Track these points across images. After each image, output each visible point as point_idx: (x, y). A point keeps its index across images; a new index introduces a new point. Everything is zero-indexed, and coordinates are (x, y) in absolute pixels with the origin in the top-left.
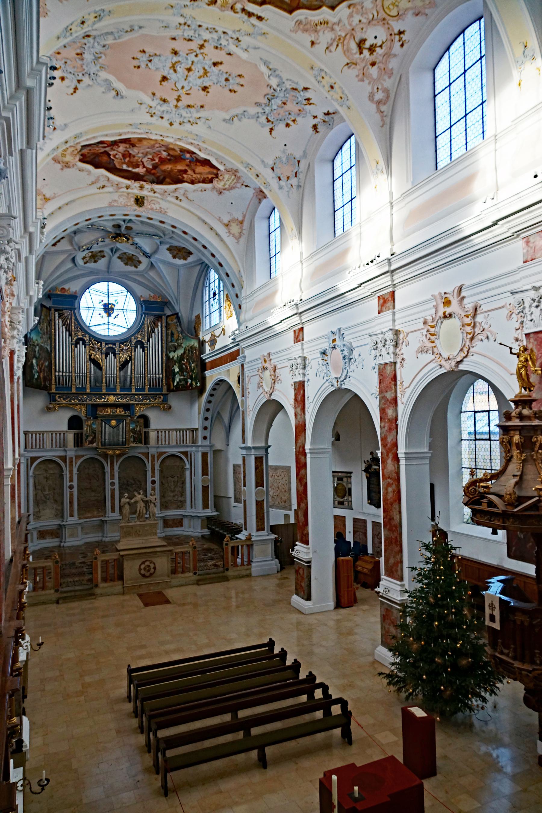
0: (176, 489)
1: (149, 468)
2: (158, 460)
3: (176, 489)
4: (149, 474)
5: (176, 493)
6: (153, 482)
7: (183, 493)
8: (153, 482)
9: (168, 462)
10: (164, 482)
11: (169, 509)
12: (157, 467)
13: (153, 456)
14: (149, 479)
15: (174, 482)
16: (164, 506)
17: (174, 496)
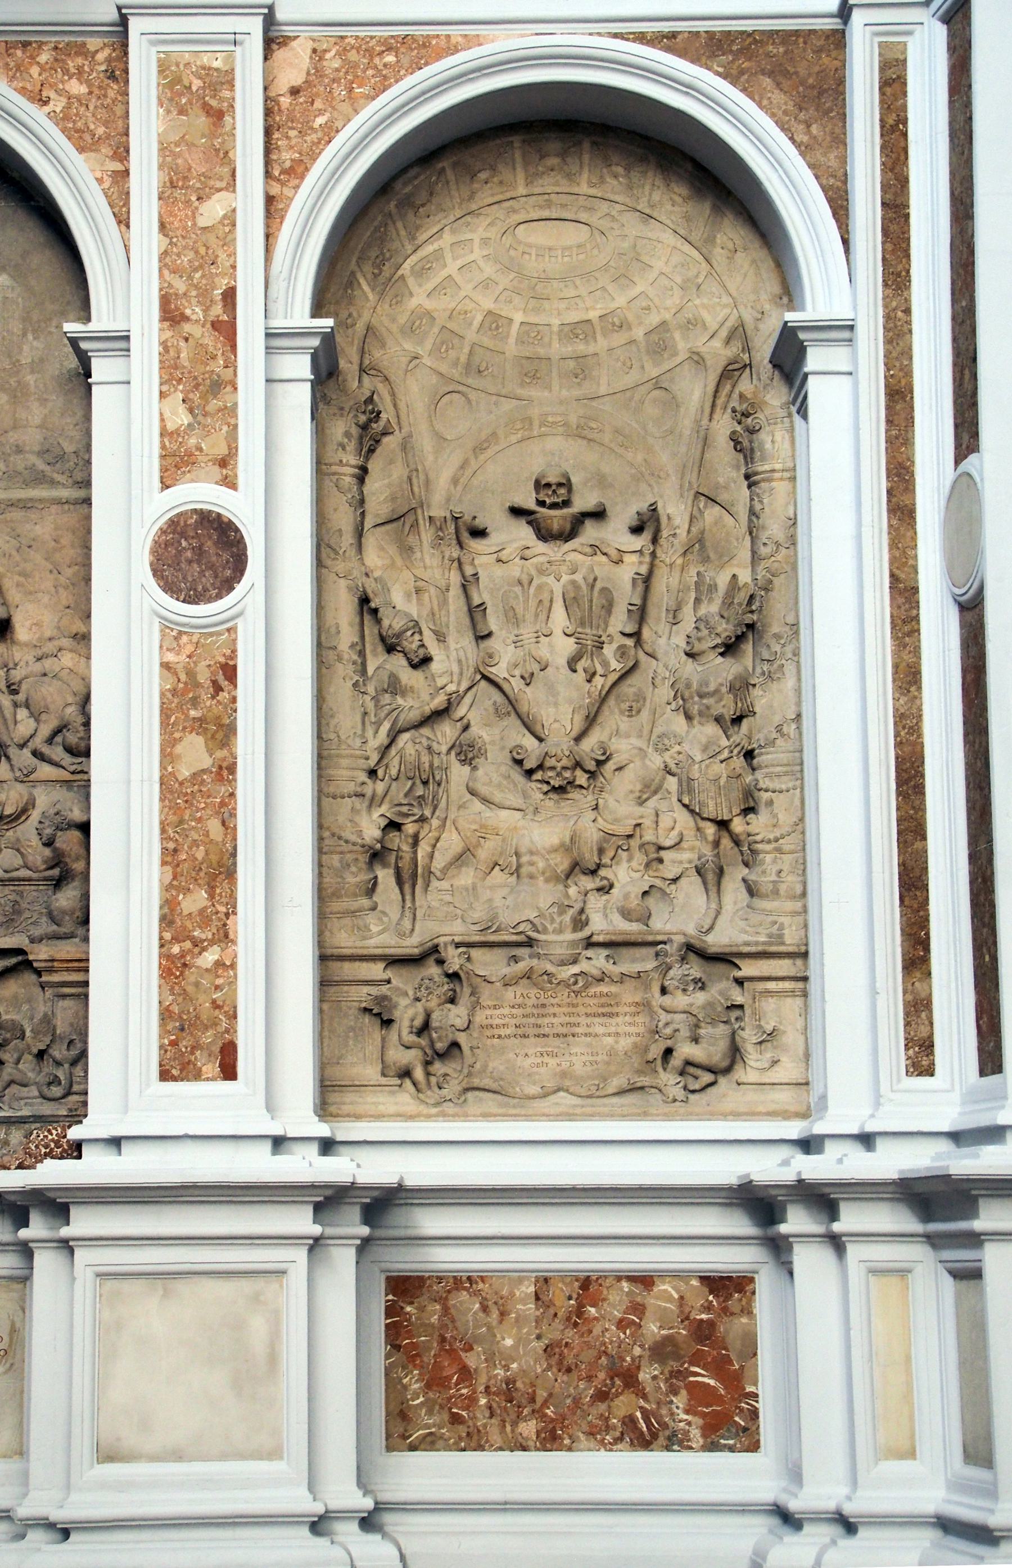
0: (619, 736)
1: (126, 284)
2: (281, 174)
3: (619, 736)
4: (128, 416)
5: (619, 804)
6: (203, 554)
7: (740, 826)
8: (203, 554)
9: (482, 261)
10: (400, 603)
11: (504, 1095)
12: (276, 284)
13: (200, 96)
14: (129, 506)
15: (588, 605)
16: (406, 1015)
17: (583, 867)
